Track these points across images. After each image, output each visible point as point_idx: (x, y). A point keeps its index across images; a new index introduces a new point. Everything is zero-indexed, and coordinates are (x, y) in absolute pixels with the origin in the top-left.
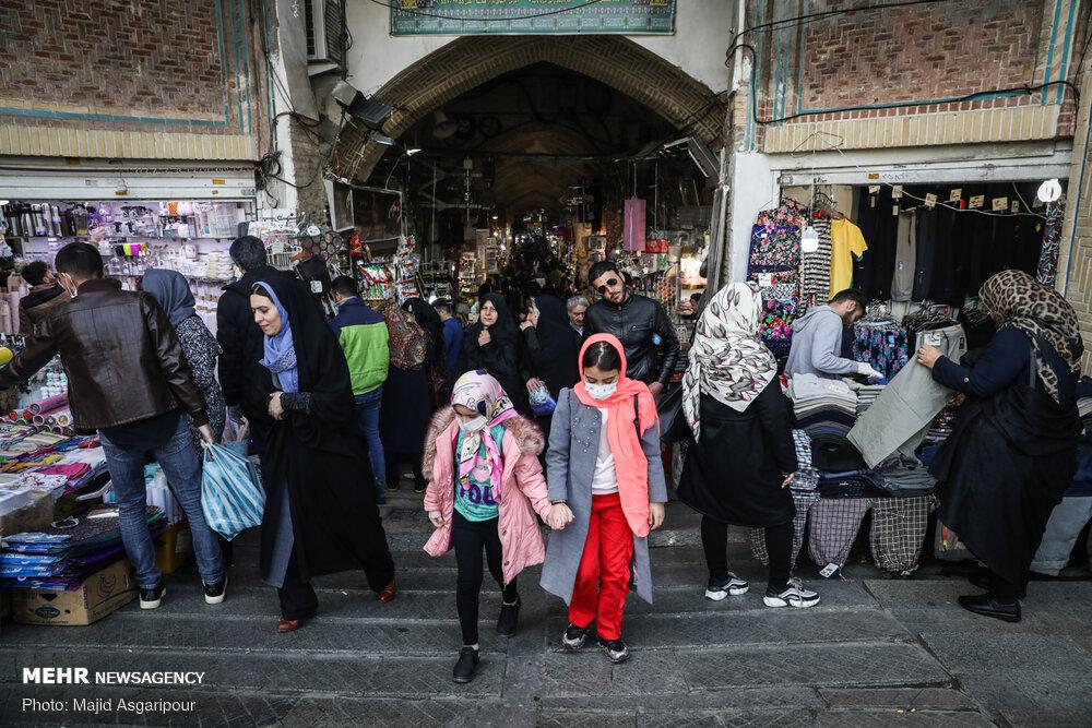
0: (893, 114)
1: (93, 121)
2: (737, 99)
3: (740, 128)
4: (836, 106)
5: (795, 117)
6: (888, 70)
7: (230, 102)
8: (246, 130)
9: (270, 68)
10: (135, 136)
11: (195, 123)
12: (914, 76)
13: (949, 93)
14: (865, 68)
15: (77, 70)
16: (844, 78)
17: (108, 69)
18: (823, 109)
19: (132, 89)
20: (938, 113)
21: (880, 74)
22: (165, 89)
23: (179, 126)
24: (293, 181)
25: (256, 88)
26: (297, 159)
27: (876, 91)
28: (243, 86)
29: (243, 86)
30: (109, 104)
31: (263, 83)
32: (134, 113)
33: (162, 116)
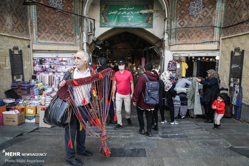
0: (192, 45)
1: (54, 44)
2: (165, 41)
3: (166, 46)
4: (182, 43)
5: (175, 45)
6: (191, 37)
7: (76, 41)
8: (78, 45)
10: (61, 47)
11: (70, 44)
12: (195, 39)
13: (201, 42)
14: (187, 37)
15: (52, 35)
16: (184, 38)
17: (56, 35)
18: (180, 44)
19: (60, 38)
20: (199, 45)
21: (189, 38)
22: (65, 38)
23: (67, 45)
25: (80, 38)
27: (189, 41)
28: (78, 38)
29: (78, 38)
30: (56, 41)
31: (81, 37)
32: (60, 43)
33: (64, 43)
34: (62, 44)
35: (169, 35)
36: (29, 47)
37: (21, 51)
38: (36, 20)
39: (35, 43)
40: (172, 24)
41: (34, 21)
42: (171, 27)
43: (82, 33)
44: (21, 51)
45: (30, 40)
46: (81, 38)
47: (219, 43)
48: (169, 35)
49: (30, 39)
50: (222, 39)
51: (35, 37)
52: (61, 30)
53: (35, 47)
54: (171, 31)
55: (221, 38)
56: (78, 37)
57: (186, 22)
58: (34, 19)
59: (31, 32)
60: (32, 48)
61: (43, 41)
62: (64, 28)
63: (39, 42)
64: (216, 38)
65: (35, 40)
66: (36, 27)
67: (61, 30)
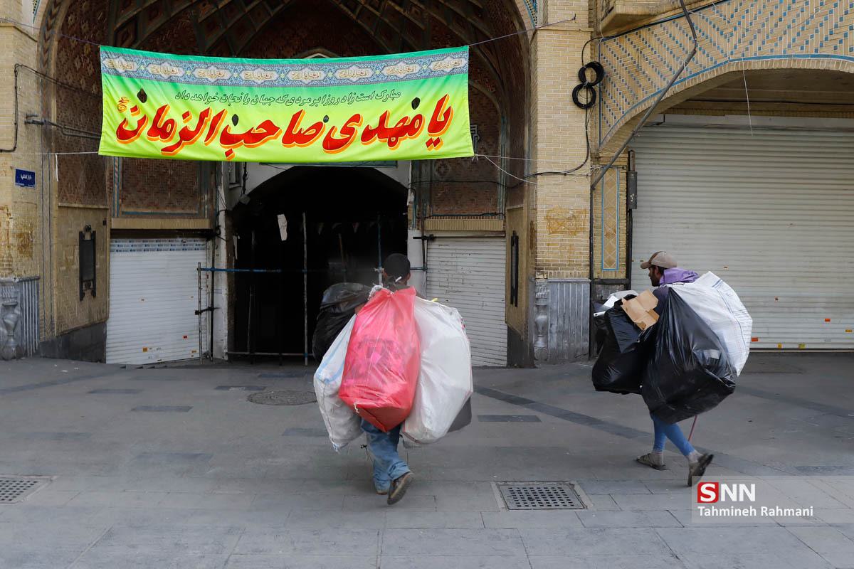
1: (153, 215)
4: (444, 214)
5: (430, 217)
6: (459, 202)
8: (206, 217)
9: (217, 191)
11: (187, 214)
23: (181, 216)
24: (224, 238)
25: (211, 200)
26: (226, 229)
28: (206, 199)
29: (206, 199)
30: (158, 208)
34: (170, 214)
35: (417, 194)
36: (105, 223)
37: (94, 232)
38: (120, 167)
39: (116, 214)
40: (423, 170)
41: (116, 169)
42: (420, 177)
43: (216, 187)
44: (94, 232)
45: (107, 209)
46: (214, 200)
47: (505, 217)
48: (417, 194)
49: (107, 207)
50: (508, 210)
51: (116, 203)
52: (169, 183)
53: (116, 223)
54: (420, 185)
55: (507, 208)
56: (206, 197)
57: (450, 168)
58: (116, 164)
59: (110, 193)
60: (111, 224)
61: (131, 210)
62: (177, 178)
63: (123, 213)
64: (500, 208)
65: (116, 208)
66: (120, 181)
67: (169, 183)
